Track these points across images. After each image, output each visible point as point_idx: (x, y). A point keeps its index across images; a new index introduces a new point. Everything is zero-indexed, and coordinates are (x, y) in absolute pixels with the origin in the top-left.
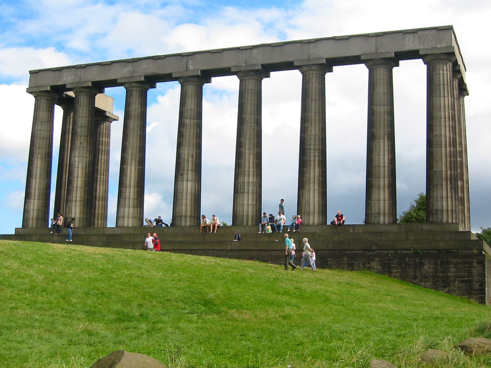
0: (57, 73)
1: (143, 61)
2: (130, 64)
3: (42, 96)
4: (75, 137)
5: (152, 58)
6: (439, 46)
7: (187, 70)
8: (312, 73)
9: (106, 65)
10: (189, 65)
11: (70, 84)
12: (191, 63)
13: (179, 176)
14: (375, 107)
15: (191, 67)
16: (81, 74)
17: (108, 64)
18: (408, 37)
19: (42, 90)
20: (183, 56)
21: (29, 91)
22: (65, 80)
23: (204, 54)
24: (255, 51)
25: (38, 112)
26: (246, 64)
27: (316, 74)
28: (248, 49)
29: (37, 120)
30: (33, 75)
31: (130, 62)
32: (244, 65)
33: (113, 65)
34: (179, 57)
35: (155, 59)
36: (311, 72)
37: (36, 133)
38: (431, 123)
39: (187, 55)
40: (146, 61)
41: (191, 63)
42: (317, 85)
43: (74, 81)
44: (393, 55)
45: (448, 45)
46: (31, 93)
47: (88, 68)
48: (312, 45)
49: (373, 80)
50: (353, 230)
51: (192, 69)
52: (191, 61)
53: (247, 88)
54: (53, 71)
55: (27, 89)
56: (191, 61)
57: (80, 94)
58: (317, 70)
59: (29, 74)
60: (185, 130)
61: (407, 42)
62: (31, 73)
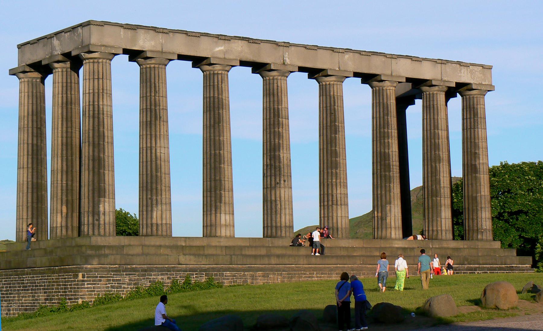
0: (129, 32)
4: (160, 123)
6: (483, 83)
10: (286, 57)
11: (151, 51)
13: (282, 182)
14: (440, 132)
15: (288, 61)
16: (163, 41)
18: (464, 69)
24: (347, 56)
25: (105, 81)
29: (105, 91)
37: (105, 110)
38: (477, 151)
43: (154, 49)
44: (454, 85)
45: (490, 83)
47: (171, 34)
48: (394, 61)
49: (437, 104)
50: (432, 245)
52: (287, 53)
53: (339, 95)
56: (287, 53)
57: (161, 66)
60: (284, 131)
61: (462, 74)
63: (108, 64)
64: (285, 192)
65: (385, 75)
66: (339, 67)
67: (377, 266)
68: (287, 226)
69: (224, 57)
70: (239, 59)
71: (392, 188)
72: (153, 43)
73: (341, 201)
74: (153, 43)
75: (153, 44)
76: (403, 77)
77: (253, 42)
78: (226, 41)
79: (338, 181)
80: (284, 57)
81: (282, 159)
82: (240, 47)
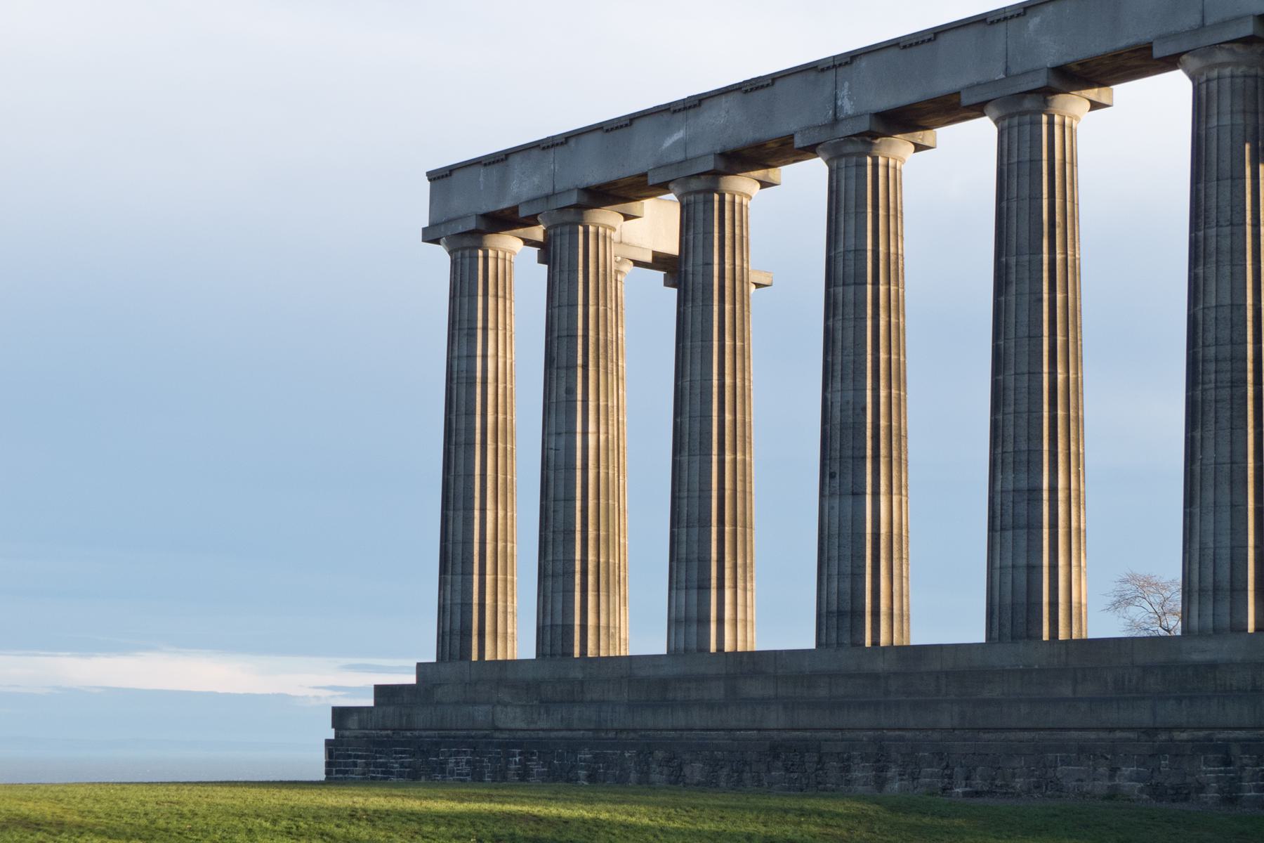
0: (494, 170)
1: (715, 101)
2: (680, 116)
3: (465, 248)
5: (737, 89)
7: (836, 121)
8: (1219, 78)
9: (617, 128)
11: (530, 201)
12: (845, 92)
15: (847, 107)
16: (557, 168)
17: (621, 126)
19: (460, 229)
20: (823, 70)
21: (430, 236)
22: (515, 190)
23: (884, 54)
26: (1006, 75)
27: (1232, 77)
28: (1012, 17)
30: (438, 182)
31: (680, 110)
32: (1002, 76)
33: (637, 124)
34: (812, 76)
35: (746, 91)
36: (1215, 73)
39: (834, 66)
40: (723, 99)
41: (845, 92)
42: (1239, 120)
46: (436, 241)
47: (572, 142)
51: (849, 112)
52: (847, 84)
54: (485, 165)
55: (424, 230)
56: (847, 84)
58: (1237, 64)
59: (429, 183)
62: (434, 177)
63: (467, 261)
64: (832, 508)
65: (1164, 38)
66: (1006, 69)
67: (1236, 740)
68: (833, 613)
69: (684, 156)
70: (718, 149)
71: (1198, 444)
72: (536, 179)
73: (1001, 516)
74: (536, 179)
75: (536, 183)
76: (1238, 19)
77: (752, 90)
78: (691, 112)
79: (999, 450)
80: (836, 99)
81: (830, 410)
82: (723, 114)
